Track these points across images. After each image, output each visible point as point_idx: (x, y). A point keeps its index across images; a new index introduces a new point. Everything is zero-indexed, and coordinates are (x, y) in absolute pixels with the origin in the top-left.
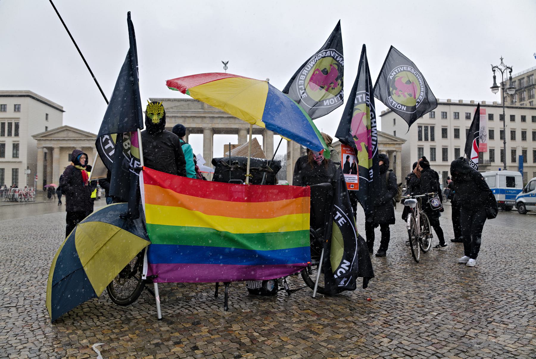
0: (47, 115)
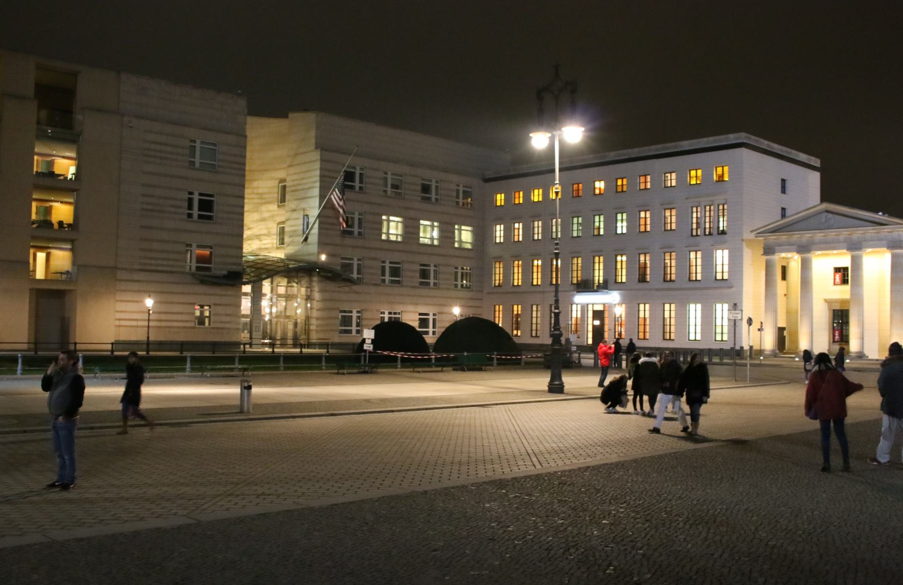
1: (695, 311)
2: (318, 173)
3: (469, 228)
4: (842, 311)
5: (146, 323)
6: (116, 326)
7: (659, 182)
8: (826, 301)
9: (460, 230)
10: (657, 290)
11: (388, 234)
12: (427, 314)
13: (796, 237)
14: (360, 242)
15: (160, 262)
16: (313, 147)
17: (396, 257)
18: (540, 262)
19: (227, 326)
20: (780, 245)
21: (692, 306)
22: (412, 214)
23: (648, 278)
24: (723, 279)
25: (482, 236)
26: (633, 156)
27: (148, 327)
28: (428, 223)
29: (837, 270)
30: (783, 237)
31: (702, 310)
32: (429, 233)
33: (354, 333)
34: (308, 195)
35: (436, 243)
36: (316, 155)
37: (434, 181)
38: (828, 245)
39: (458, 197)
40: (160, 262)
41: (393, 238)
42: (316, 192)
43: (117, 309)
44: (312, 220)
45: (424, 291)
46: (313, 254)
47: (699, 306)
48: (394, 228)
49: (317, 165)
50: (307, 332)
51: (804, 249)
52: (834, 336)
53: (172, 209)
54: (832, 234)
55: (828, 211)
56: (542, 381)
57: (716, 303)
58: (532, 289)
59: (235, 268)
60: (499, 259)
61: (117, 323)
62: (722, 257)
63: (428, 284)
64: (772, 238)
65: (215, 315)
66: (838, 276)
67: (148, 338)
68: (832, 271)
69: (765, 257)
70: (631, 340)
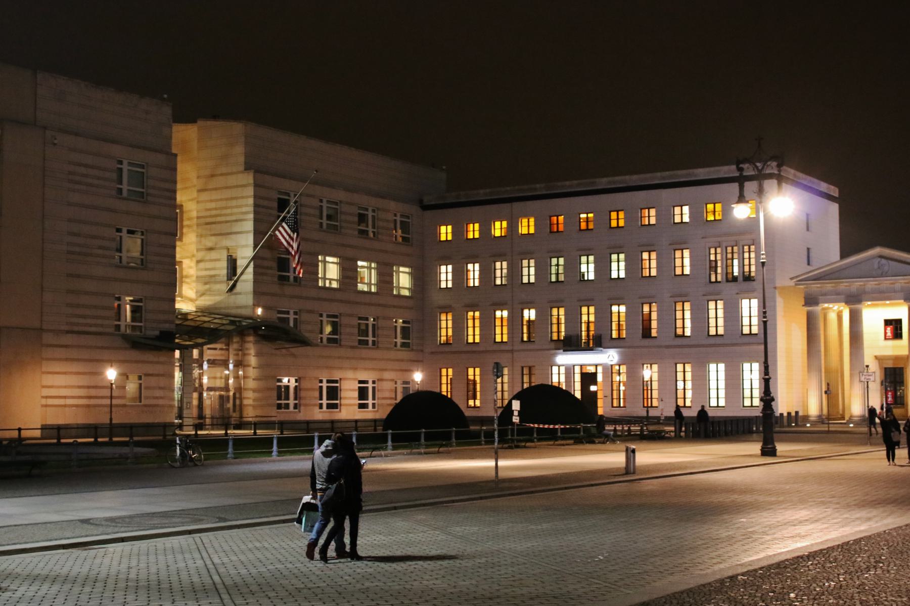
1: (717, 372)
2: (251, 201)
3: (407, 270)
4: (894, 369)
5: (108, 402)
6: (43, 406)
7: (665, 216)
8: (876, 357)
9: (398, 272)
10: (668, 347)
11: (324, 279)
13: (844, 285)
15: (89, 321)
16: (242, 168)
17: (335, 309)
18: (505, 314)
19: (161, 402)
20: (825, 295)
21: (713, 367)
22: (350, 253)
23: (654, 333)
24: (751, 334)
25: (424, 278)
26: (631, 184)
27: (111, 405)
28: (365, 264)
29: (888, 322)
30: (829, 286)
31: (726, 371)
32: (367, 275)
34: (235, 229)
35: (373, 289)
36: (249, 178)
37: (370, 209)
38: (881, 296)
40: (89, 321)
42: (249, 225)
43: (45, 383)
44: (241, 263)
45: (364, 353)
46: (246, 307)
47: (722, 366)
48: (330, 271)
49: (250, 191)
50: (239, 408)
51: (854, 299)
52: (887, 398)
53: (100, 252)
54: (886, 283)
55: (881, 257)
56: (755, 448)
57: (709, 362)
58: (496, 347)
59: (166, 327)
60: (446, 309)
61: (44, 402)
62: (749, 309)
63: (367, 342)
64: (815, 287)
65: (147, 388)
66: (889, 329)
67: (111, 419)
68: (883, 323)
69: (807, 308)
70: (703, 407)
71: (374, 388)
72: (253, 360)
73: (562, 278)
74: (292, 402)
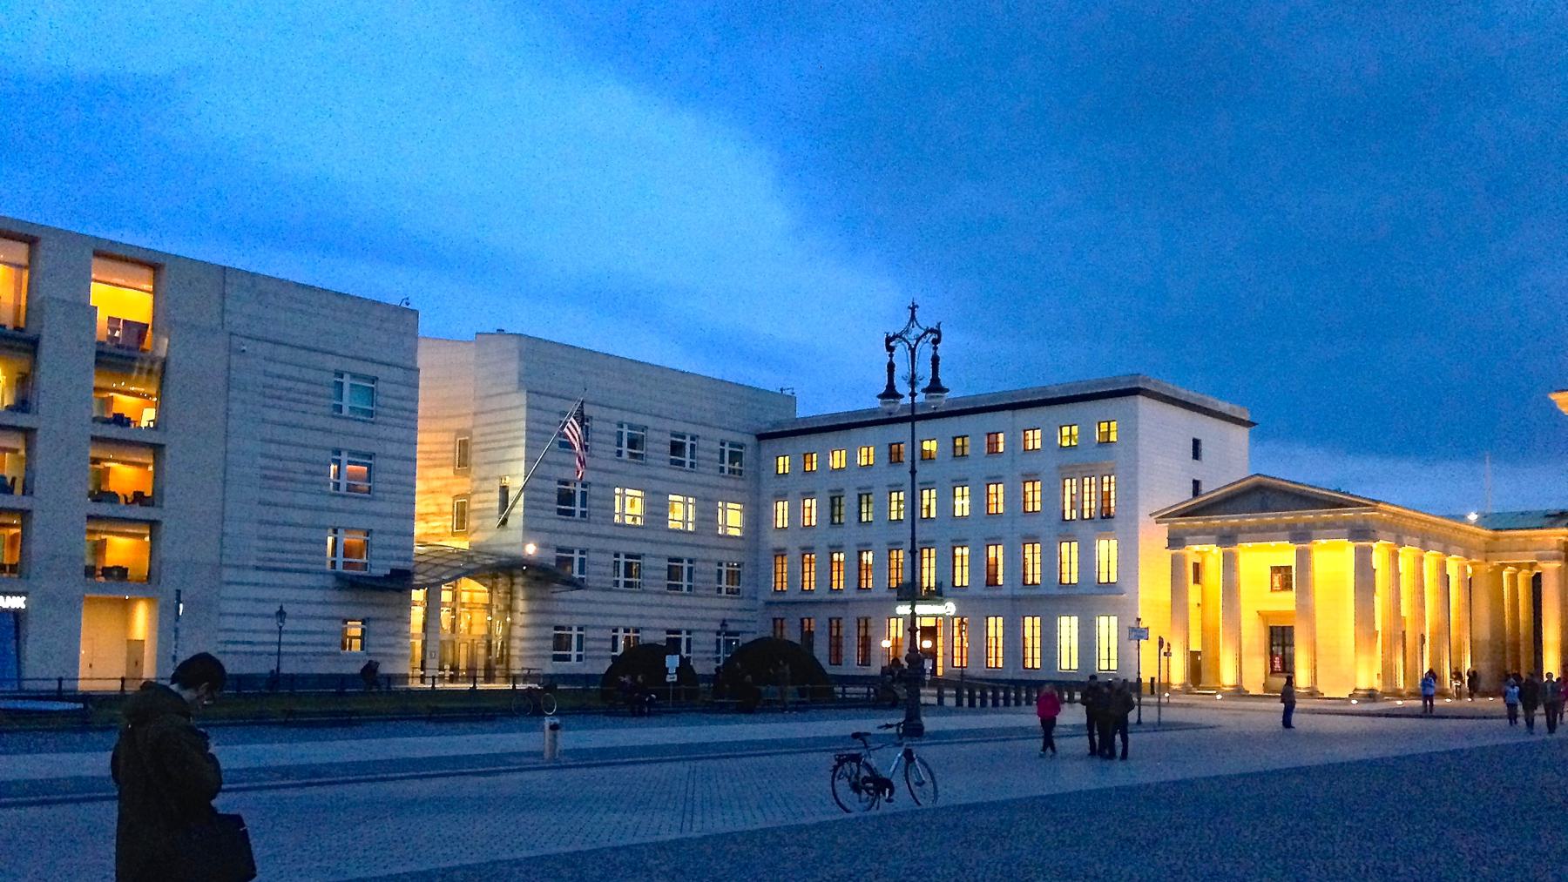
0: (1196, 443)
2: (523, 424)
3: (738, 506)
4: (1283, 628)
5: (275, 648)
9: (725, 510)
12: (679, 632)
13: (1216, 521)
14: (583, 527)
19: (390, 651)
22: (657, 485)
25: (756, 519)
27: (279, 653)
28: (680, 498)
29: (1276, 570)
30: (1199, 522)
32: (681, 513)
33: (574, 658)
34: (509, 456)
35: (690, 528)
36: (521, 399)
38: (1263, 533)
39: (722, 461)
41: (628, 520)
42: (521, 452)
44: (512, 494)
46: (513, 544)
48: (630, 506)
49: (523, 413)
50: (505, 658)
51: (1227, 538)
52: (1272, 664)
54: (1269, 518)
59: (401, 565)
64: (1182, 523)
66: (1276, 579)
68: (1269, 572)
69: (1169, 552)
71: (688, 641)
72: (521, 605)
73: (933, 515)
74: (574, 653)
